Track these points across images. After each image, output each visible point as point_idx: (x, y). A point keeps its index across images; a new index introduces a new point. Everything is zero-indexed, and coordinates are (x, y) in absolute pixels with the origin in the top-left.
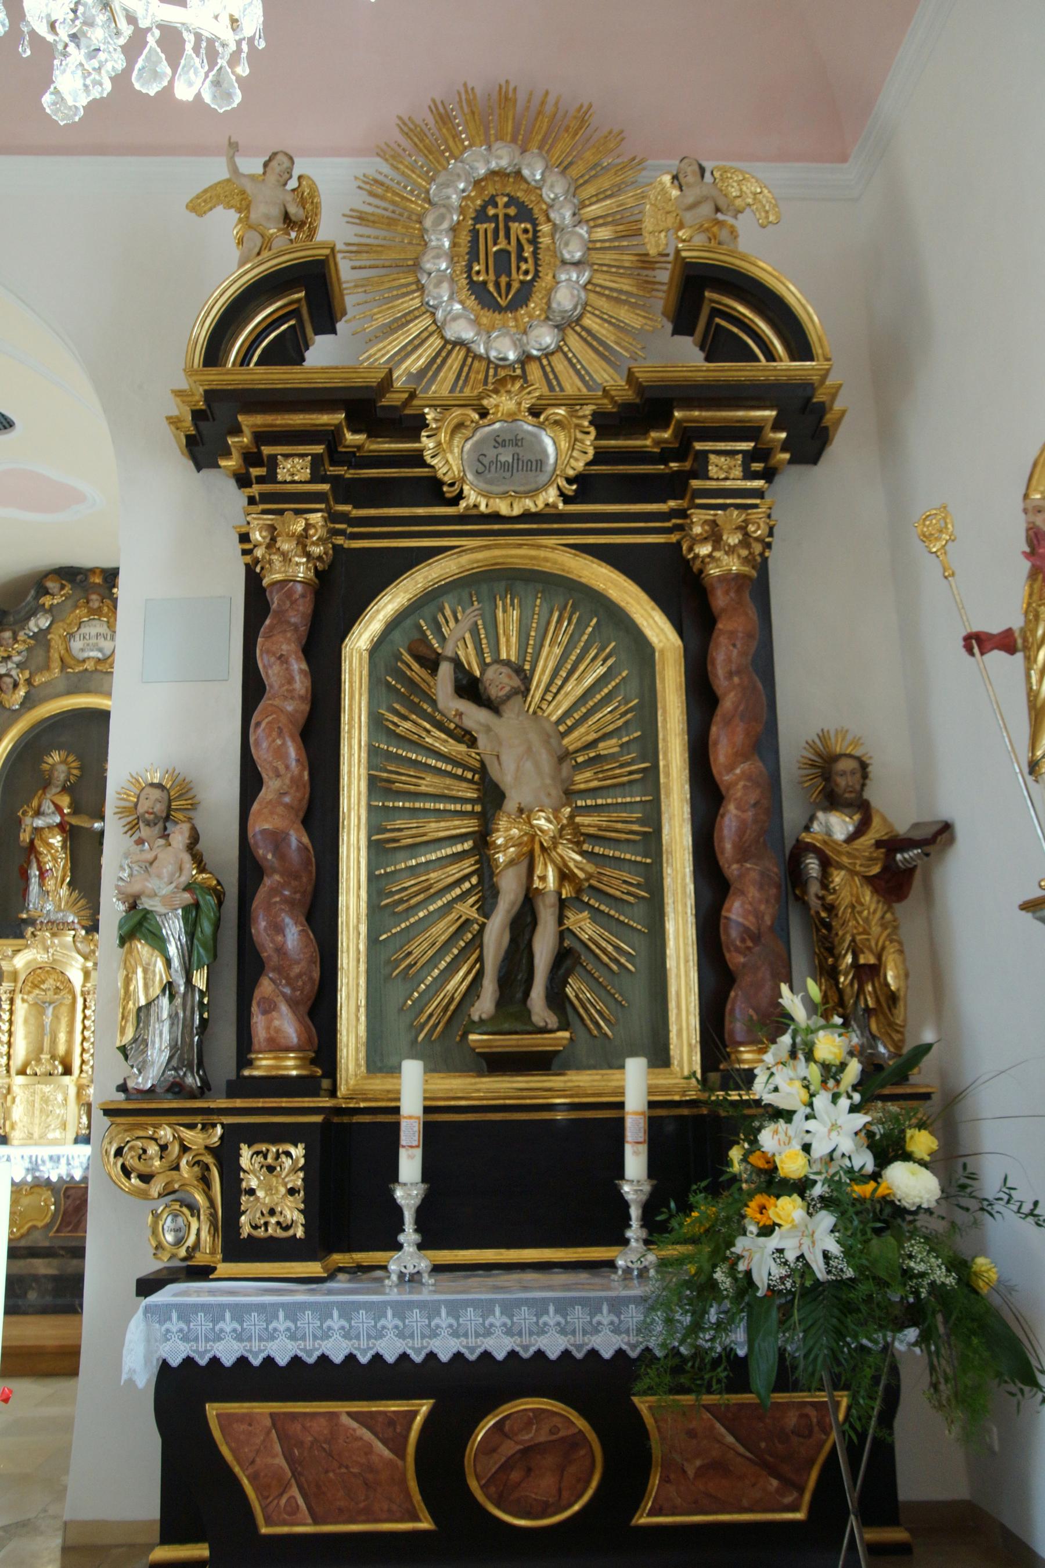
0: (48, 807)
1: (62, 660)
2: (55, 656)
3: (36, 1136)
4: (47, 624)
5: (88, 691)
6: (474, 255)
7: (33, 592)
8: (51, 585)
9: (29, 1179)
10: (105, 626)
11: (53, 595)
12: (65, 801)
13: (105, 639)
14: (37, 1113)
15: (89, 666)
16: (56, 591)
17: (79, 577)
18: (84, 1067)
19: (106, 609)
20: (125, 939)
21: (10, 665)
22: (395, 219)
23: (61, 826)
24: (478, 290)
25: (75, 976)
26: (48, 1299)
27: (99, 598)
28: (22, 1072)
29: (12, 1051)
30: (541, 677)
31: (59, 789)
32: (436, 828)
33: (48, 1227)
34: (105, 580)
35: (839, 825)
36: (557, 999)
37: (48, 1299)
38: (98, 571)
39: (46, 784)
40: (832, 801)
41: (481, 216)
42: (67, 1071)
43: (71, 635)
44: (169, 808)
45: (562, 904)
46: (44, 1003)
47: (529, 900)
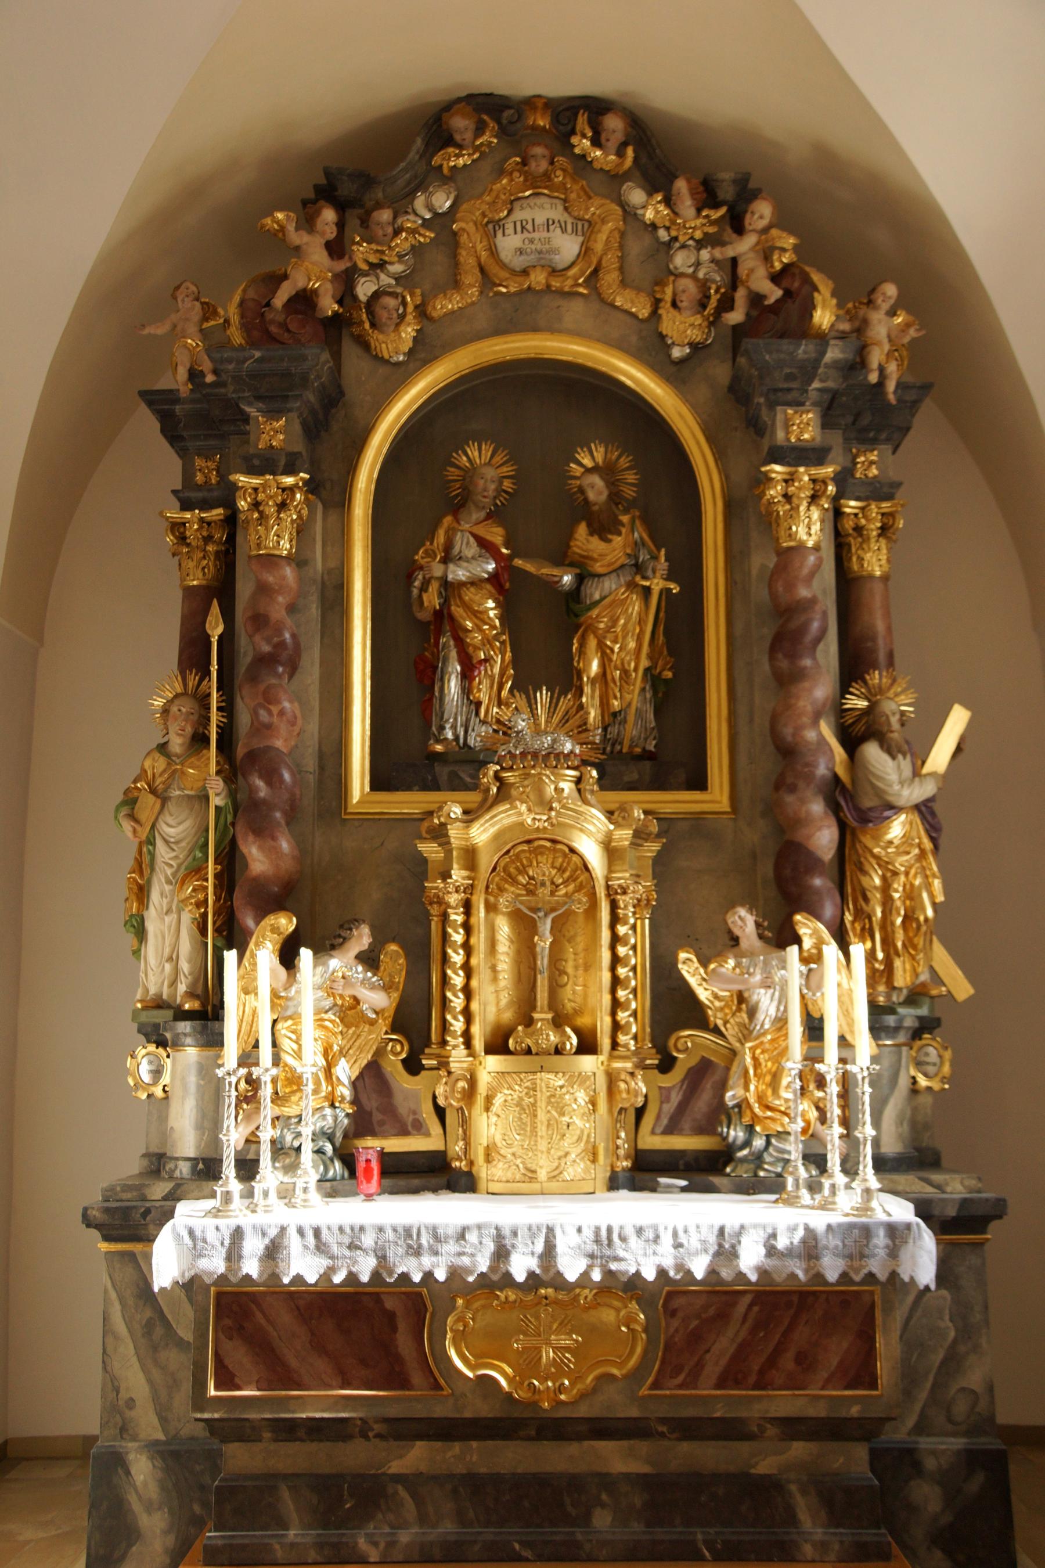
1: (482, 270)
2: (467, 260)
3: (542, 1175)
4: (448, 204)
5: (535, 329)
7: (419, 142)
8: (461, 124)
9: (596, 1276)
10: (560, 208)
11: (460, 147)
12: (496, 535)
13: (564, 231)
14: (542, 1130)
15: (538, 279)
16: (469, 135)
17: (507, 114)
18: (622, 1038)
19: (559, 178)
21: (385, 280)
23: (494, 579)
26: (637, 1529)
27: (546, 152)
28: (498, 1045)
29: (474, 1006)
31: (482, 514)
33: (636, 1376)
34: (556, 120)
37: (637, 1529)
38: (540, 104)
39: (458, 506)
42: (587, 1046)
43: (493, 227)
46: (535, 910)
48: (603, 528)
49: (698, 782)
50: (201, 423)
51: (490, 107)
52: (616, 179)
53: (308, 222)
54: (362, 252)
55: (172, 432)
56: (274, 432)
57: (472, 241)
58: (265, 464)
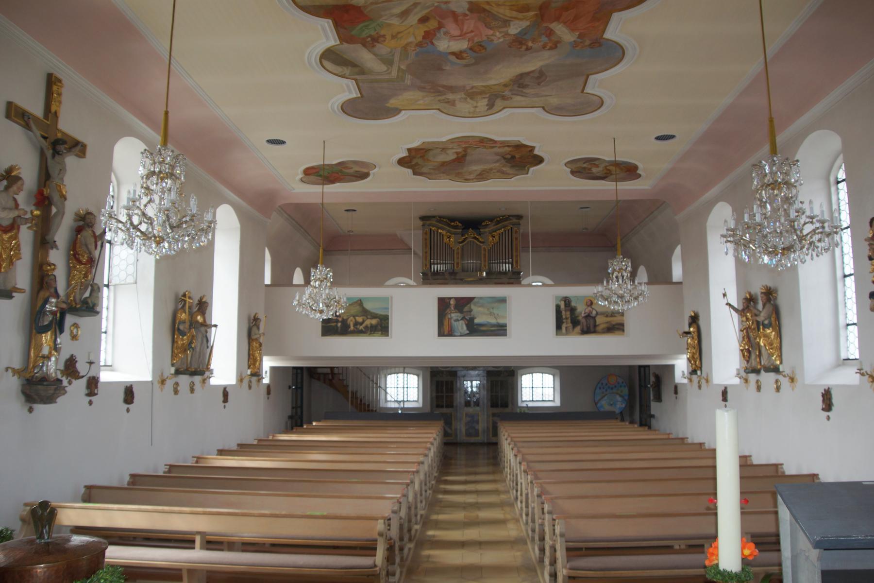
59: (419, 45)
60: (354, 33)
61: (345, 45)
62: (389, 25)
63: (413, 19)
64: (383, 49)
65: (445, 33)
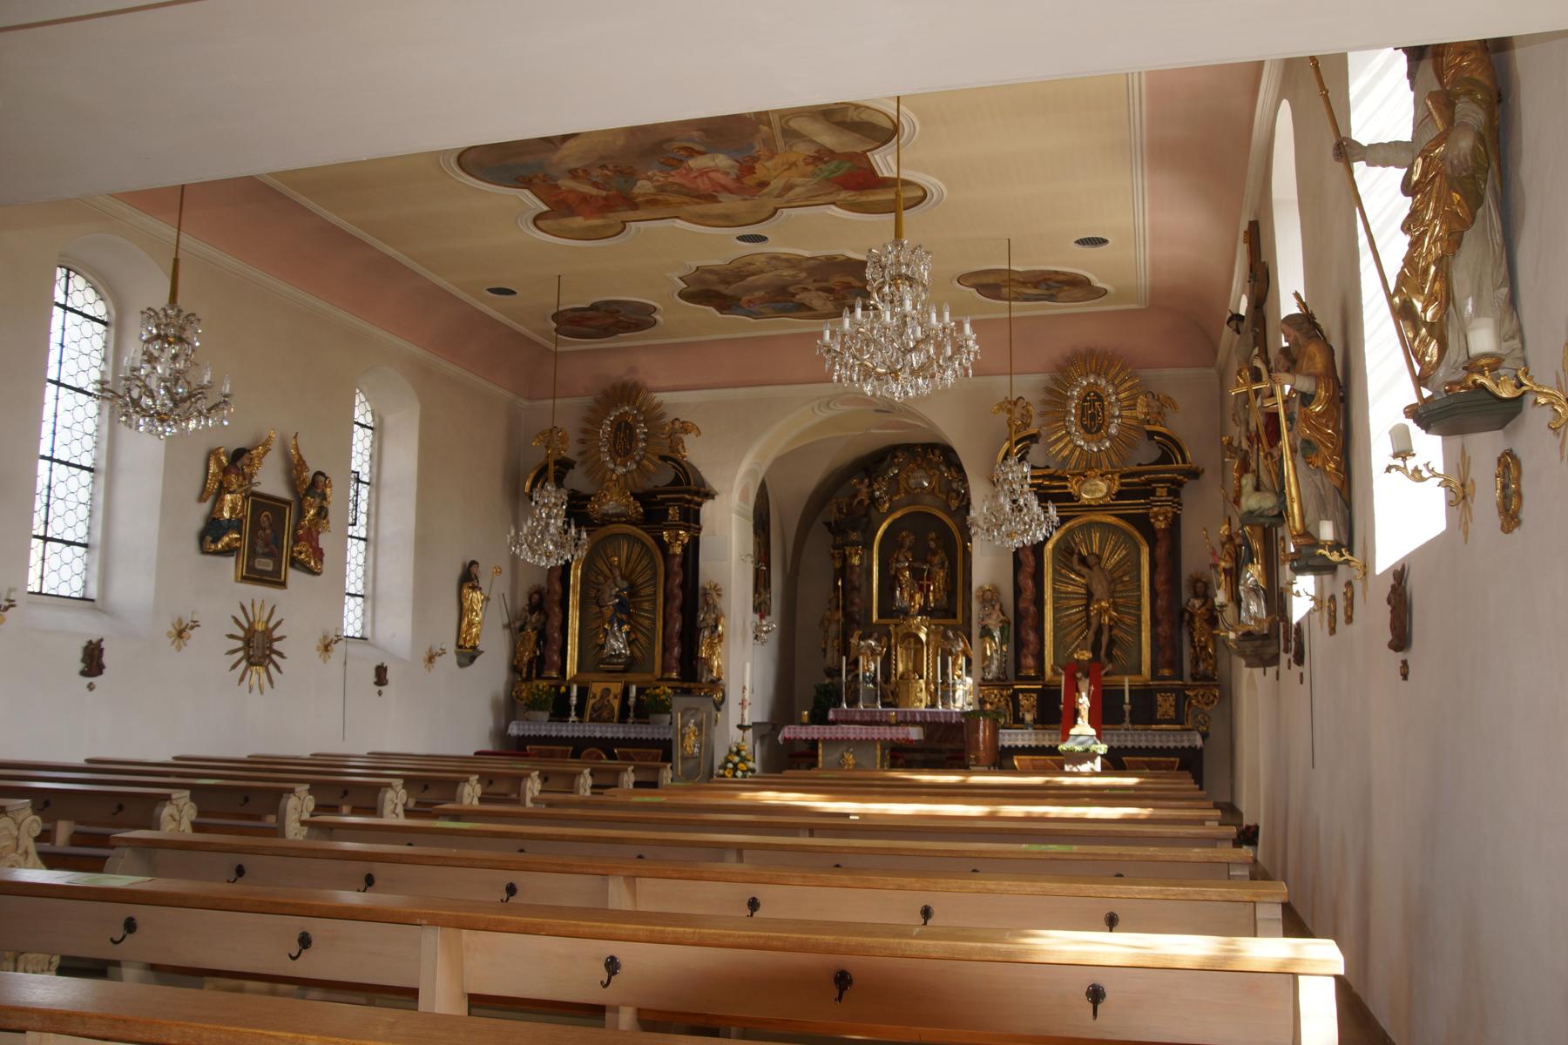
0: (901, 558)
6: (1083, 414)
12: (909, 555)
20: (982, 636)
22: (1055, 398)
24: (1084, 427)
25: (923, 637)
30: (1106, 555)
32: (1073, 603)
35: (1197, 603)
36: (1109, 655)
39: (901, 546)
40: (1196, 596)
41: (1085, 400)
42: (921, 677)
44: (990, 597)
45: (1111, 628)
47: (1100, 626)
48: (934, 553)
49: (954, 616)
50: (837, 529)
51: (908, 448)
52: (938, 464)
53: (862, 482)
54: (876, 486)
55: (830, 530)
56: (854, 536)
57: (903, 483)
58: (854, 544)
59: (756, 159)
60: (848, 165)
61: (859, 150)
62: (804, 176)
63: (776, 184)
64: (802, 150)
65: (727, 174)
